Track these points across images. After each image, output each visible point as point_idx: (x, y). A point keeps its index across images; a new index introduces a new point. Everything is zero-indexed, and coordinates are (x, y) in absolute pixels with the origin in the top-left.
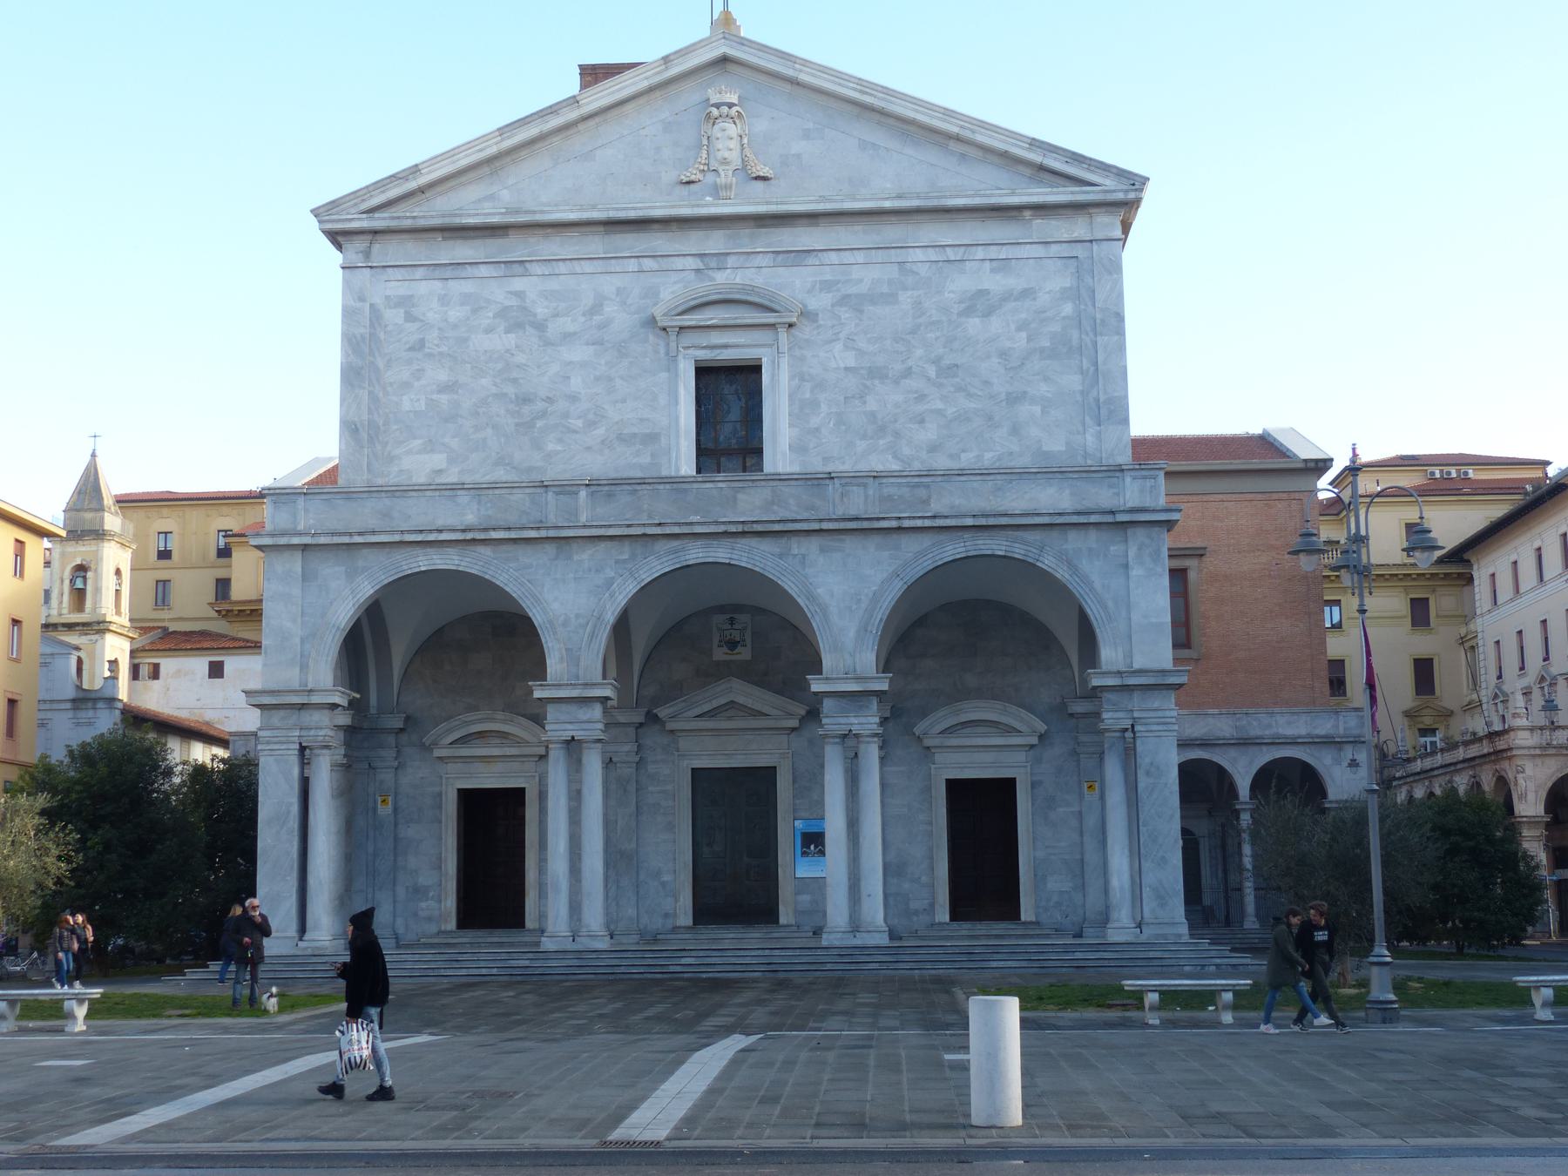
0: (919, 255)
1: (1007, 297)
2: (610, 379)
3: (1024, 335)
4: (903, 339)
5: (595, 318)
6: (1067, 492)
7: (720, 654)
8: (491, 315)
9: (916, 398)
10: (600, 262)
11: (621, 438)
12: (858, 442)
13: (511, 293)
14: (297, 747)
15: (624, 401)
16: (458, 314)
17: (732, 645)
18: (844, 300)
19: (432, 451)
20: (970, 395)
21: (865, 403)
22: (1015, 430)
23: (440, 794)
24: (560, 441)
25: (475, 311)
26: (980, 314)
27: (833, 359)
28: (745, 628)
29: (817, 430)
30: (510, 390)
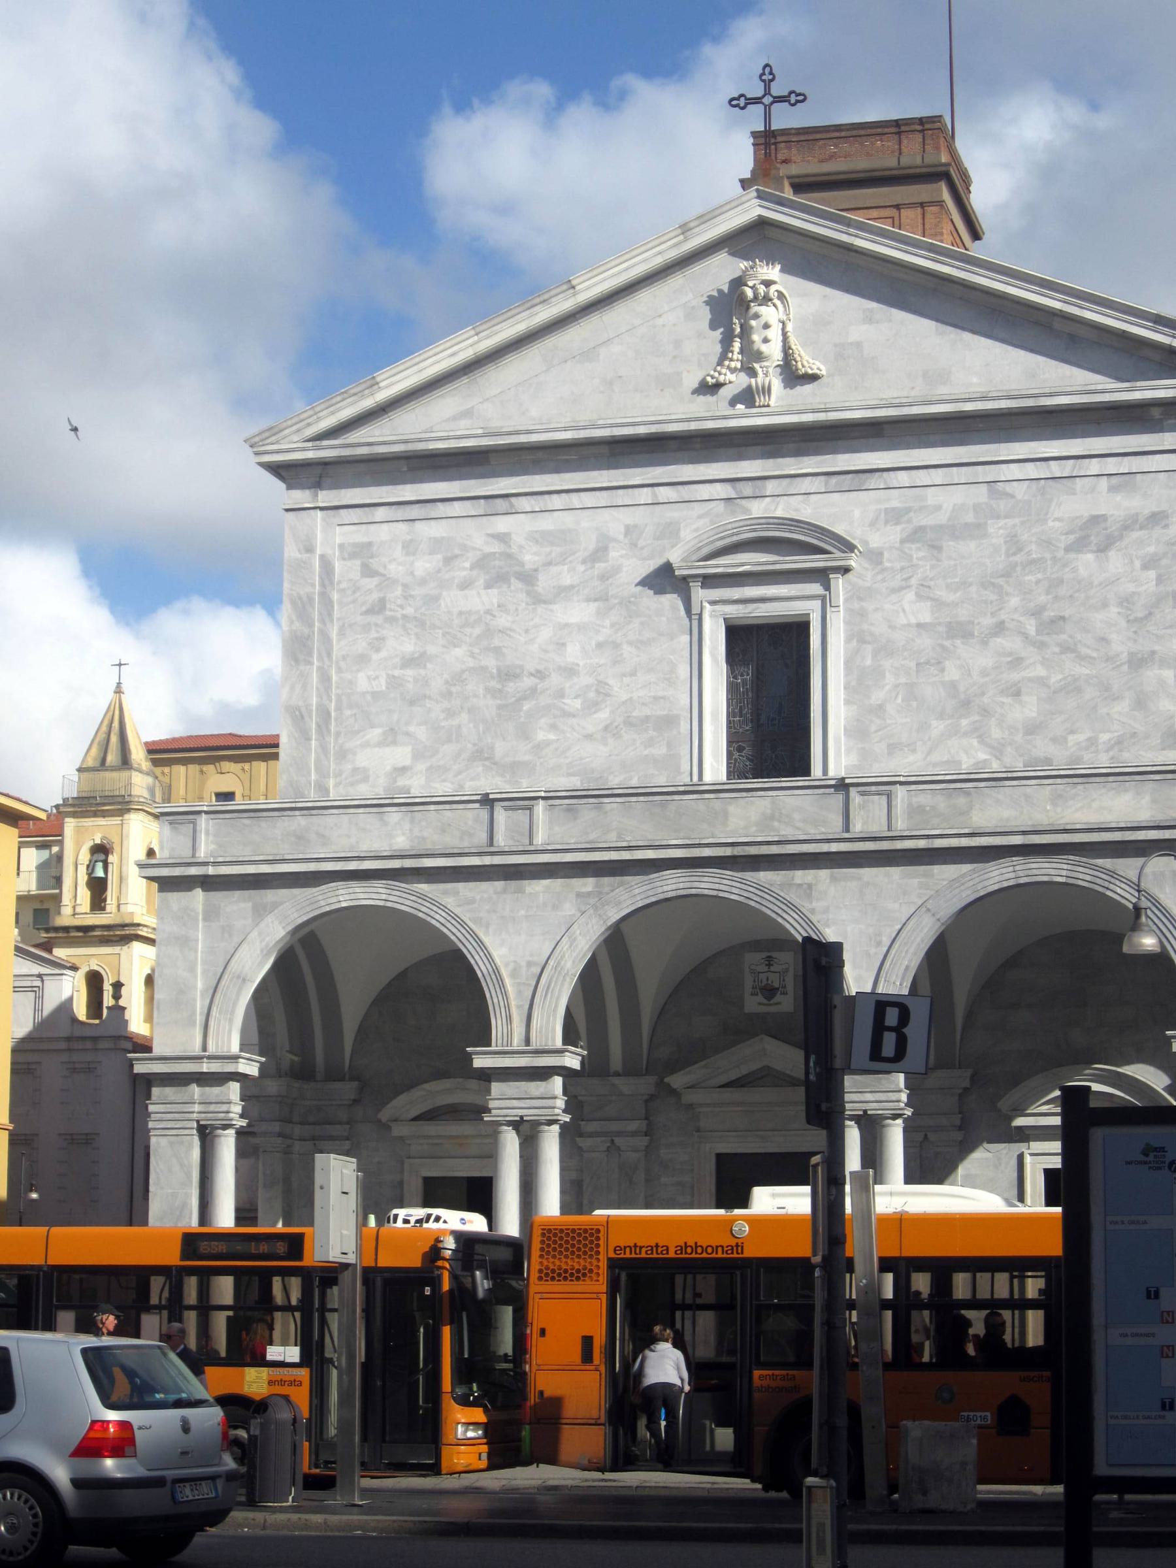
0: (1014, 471)
1: (1131, 523)
2: (616, 646)
3: (1152, 574)
4: (993, 584)
5: (597, 565)
6: (1147, 798)
7: (753, 1004)
8: (467, 565)
9: (1008, 663)
10: (604, 493)
11: (629, 723)
12: (934, 723)
13: (493, 536)
14: (195, 1125)
15: (633, 674)
16: (428, 565)
17: (770, 992)
18: (916, 535)
19: (394, 743)
20: (1081, 658)
21: (943, 670)
22: (1141, 703)
23: (401, 1183)
24: (553, 727)
25: (448, 561)
26: (1095, 549)
27: (902, 614)
28: (787, 970)
29: (881, 707)
30: (490, 662)
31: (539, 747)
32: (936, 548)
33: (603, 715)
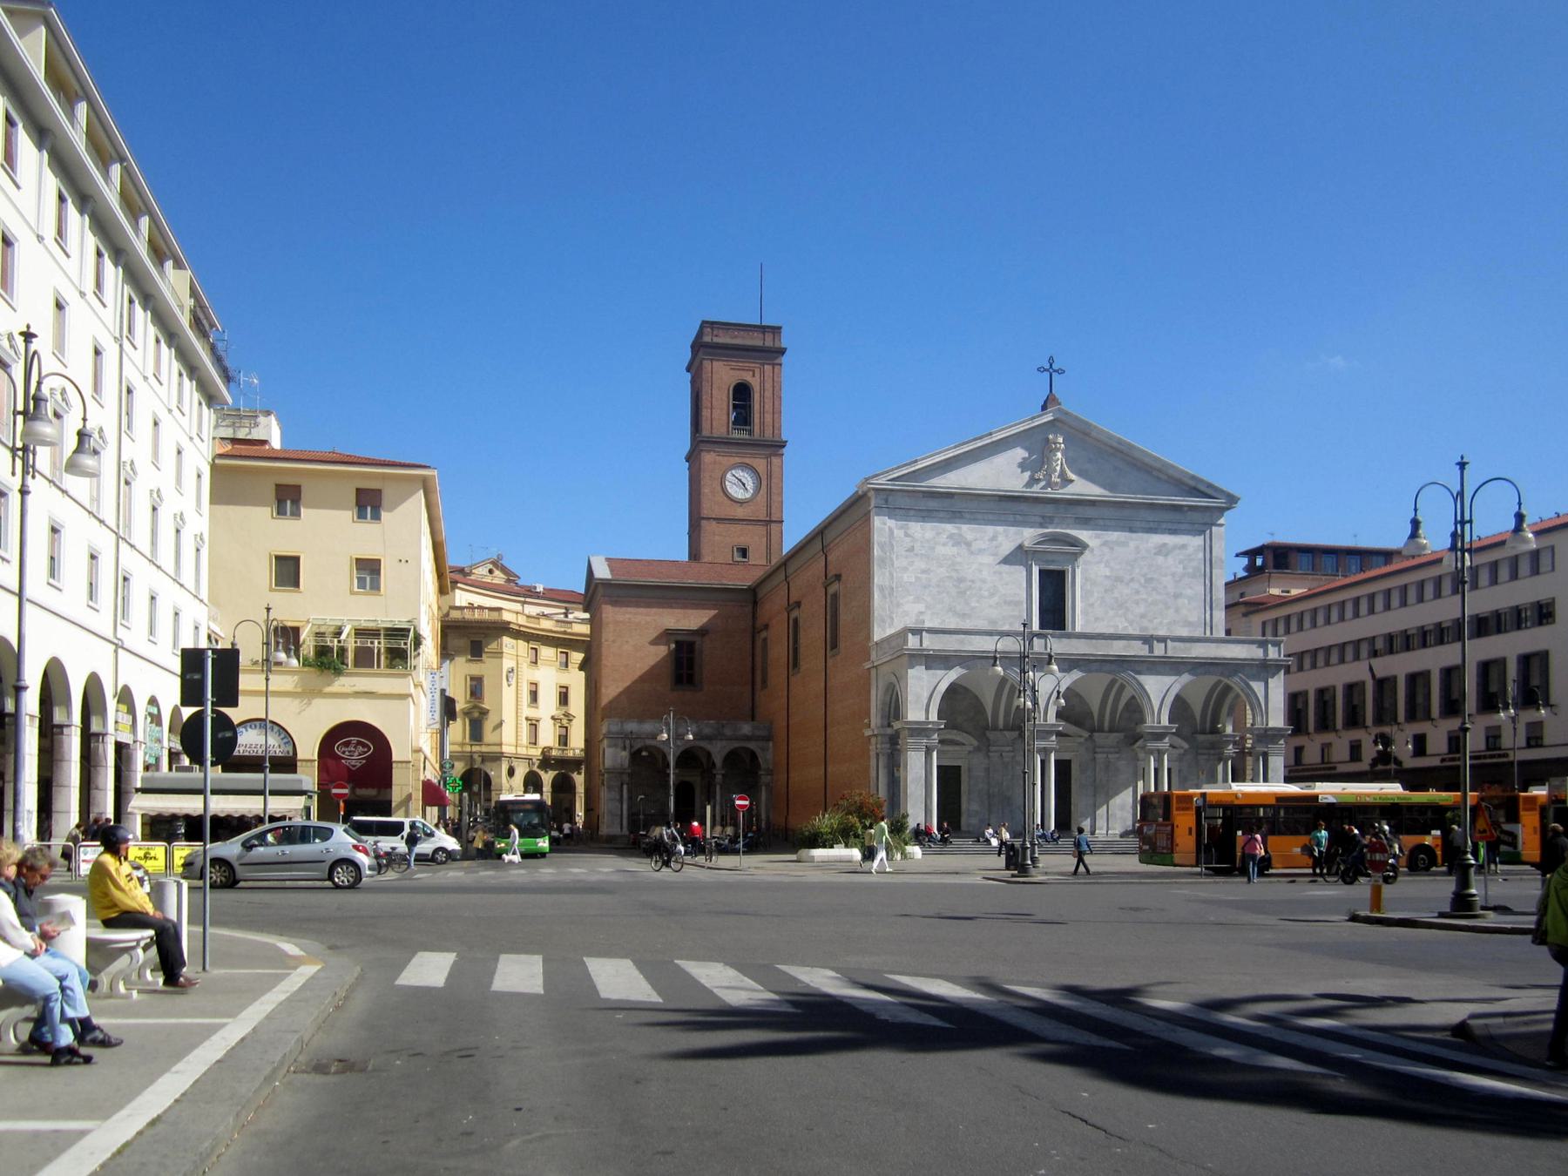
1: (1175, 547)
8: (945, 536)
11: (1005, 602)
15: (1007, 584)
22: (1177, 611)
24: (978, 602)
30: (954, 575)
31: (973, 608)
32: (1112, 549)
33: (996, 599)
